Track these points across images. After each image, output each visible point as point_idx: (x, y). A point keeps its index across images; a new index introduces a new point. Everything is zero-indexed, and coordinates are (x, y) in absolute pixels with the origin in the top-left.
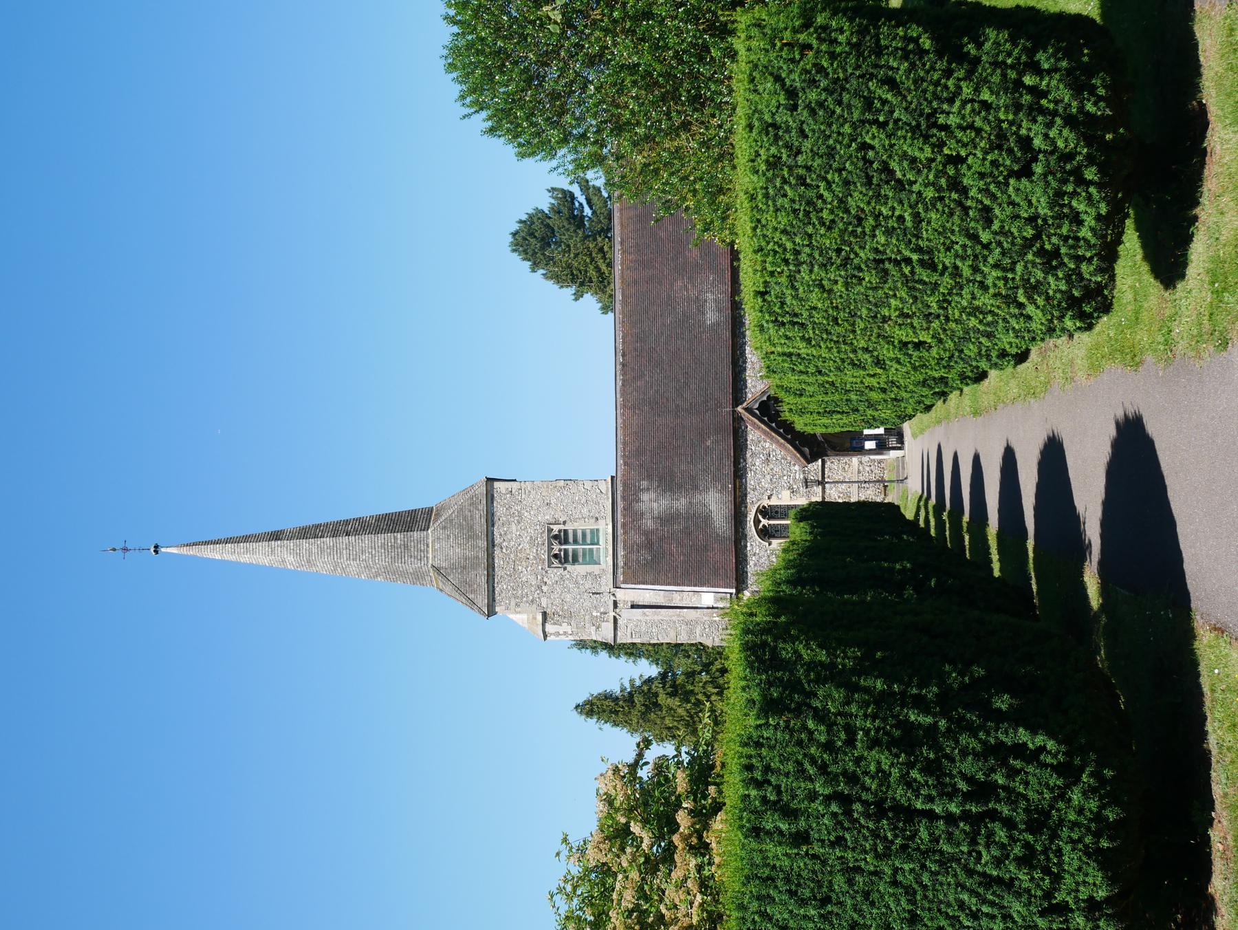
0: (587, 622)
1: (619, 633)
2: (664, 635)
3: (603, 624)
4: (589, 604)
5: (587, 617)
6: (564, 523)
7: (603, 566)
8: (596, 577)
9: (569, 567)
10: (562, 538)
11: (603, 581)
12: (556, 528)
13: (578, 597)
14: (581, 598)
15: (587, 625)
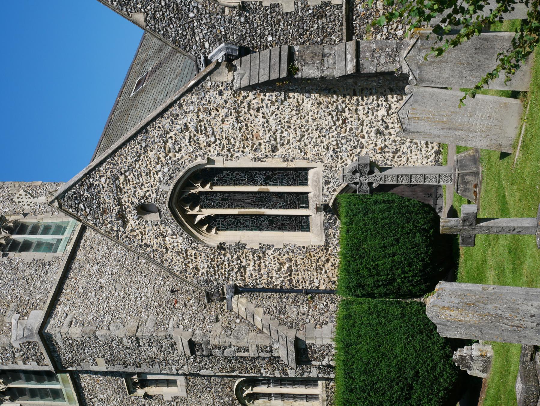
0: (10, 308)
1: (52, 321)
2: (120, 325)
3: (33, 313)
4: (22, 291)
5: (12, 305)
6: (25, 215)
7: (59, 253)
8: (42, 264)
9: (11, 254)
10: (21, 228)
11: (54, 267)
12: (11, 218)
13: (11, 282)
14: (13, 284)
15: (8, 313)
